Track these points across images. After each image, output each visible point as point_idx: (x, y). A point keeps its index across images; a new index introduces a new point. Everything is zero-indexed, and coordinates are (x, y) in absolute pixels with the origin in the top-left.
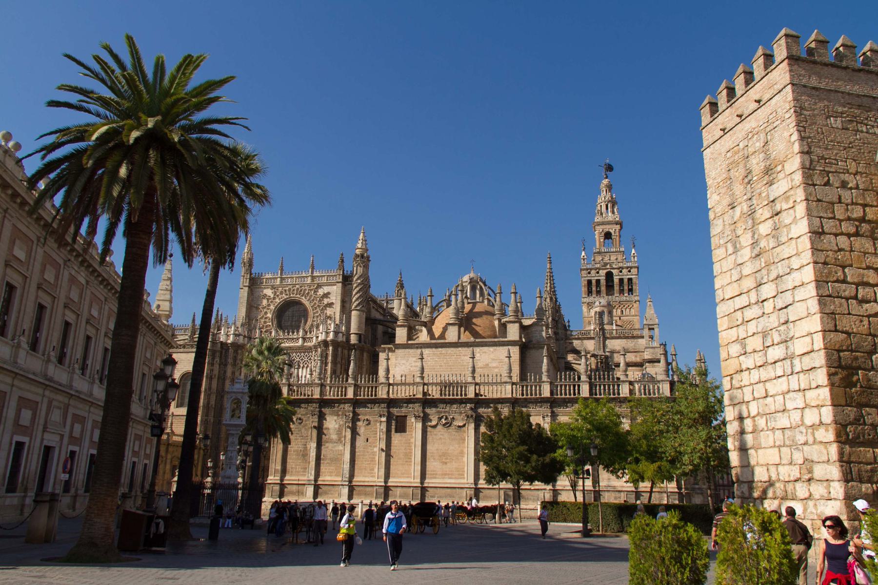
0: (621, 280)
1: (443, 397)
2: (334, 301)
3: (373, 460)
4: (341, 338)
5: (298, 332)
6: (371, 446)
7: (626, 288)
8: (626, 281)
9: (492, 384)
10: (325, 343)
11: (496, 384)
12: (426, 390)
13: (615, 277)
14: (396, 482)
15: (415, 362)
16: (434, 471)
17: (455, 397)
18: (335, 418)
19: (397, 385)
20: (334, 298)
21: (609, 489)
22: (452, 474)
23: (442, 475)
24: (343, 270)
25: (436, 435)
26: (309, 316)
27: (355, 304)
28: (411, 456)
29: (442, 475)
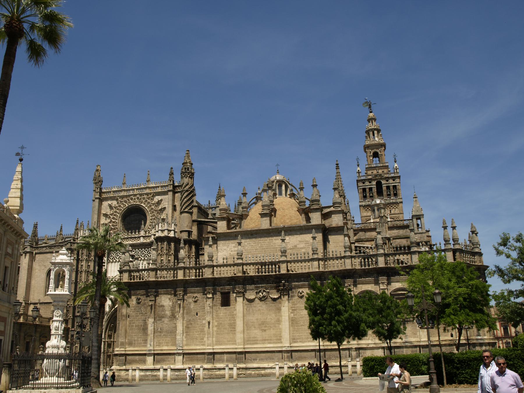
0: (388, 187)
1: (260, 274)
2: (166, 206)
3: (202, 331)
4: (172, 234)
5: (139, 232)
6: (200, 319)
7: (392, 193)
8: (391, 188)
9: (301, 261)
10: (159, 240)
11: (305, 261)
12: (245, 270)
13: (383, 185)
14: (223, 349)
15: (234, 247)
16: (255, 338)
17: (271, 274)
18: (169, 296)
19: (220, 266)
20: (167, 203)
21: (407, 344)
22: (270, 340)
23: (262, 340)
24: (173, 181)
25: (255, 307)
26: (148, 219)
27: (184, 207)
28: (235, 326)
29: (262, 340)
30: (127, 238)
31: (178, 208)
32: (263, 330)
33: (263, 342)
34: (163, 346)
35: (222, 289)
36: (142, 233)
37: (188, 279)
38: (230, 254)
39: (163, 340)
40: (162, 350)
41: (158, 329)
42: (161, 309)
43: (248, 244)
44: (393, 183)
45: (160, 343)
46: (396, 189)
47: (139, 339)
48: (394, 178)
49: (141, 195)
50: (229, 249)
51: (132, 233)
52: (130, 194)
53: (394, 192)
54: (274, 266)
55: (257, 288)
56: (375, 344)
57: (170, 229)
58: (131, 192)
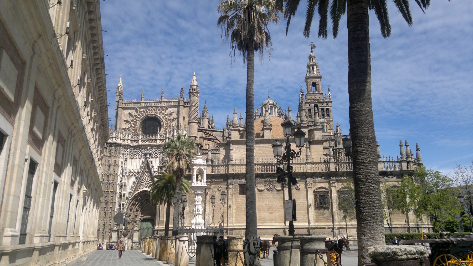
0: (323, 109)
8: (325, 110)
16: (265, 218)
22: (276, 220)
23: (270, 220)
25: (264, 195)
29: (270, 220)
30: (146, 140)
31: (187, 119)
32: (271, 212)
33: (271, 221)
35: (240, 182)
36: (159, 137)
37: (214, 174)
38: (241, 156)
41: (190, 211)
44: (327, 107)
46: (329, 111)
48: (327, 103)
49: (156, 107)
50: (240, 153)
51: (149, 136)
52: (148, 106)
53: (327, 113)
54: (273, 167)
55: (266, 182)
56: (351, 225)
58: (149, 104)
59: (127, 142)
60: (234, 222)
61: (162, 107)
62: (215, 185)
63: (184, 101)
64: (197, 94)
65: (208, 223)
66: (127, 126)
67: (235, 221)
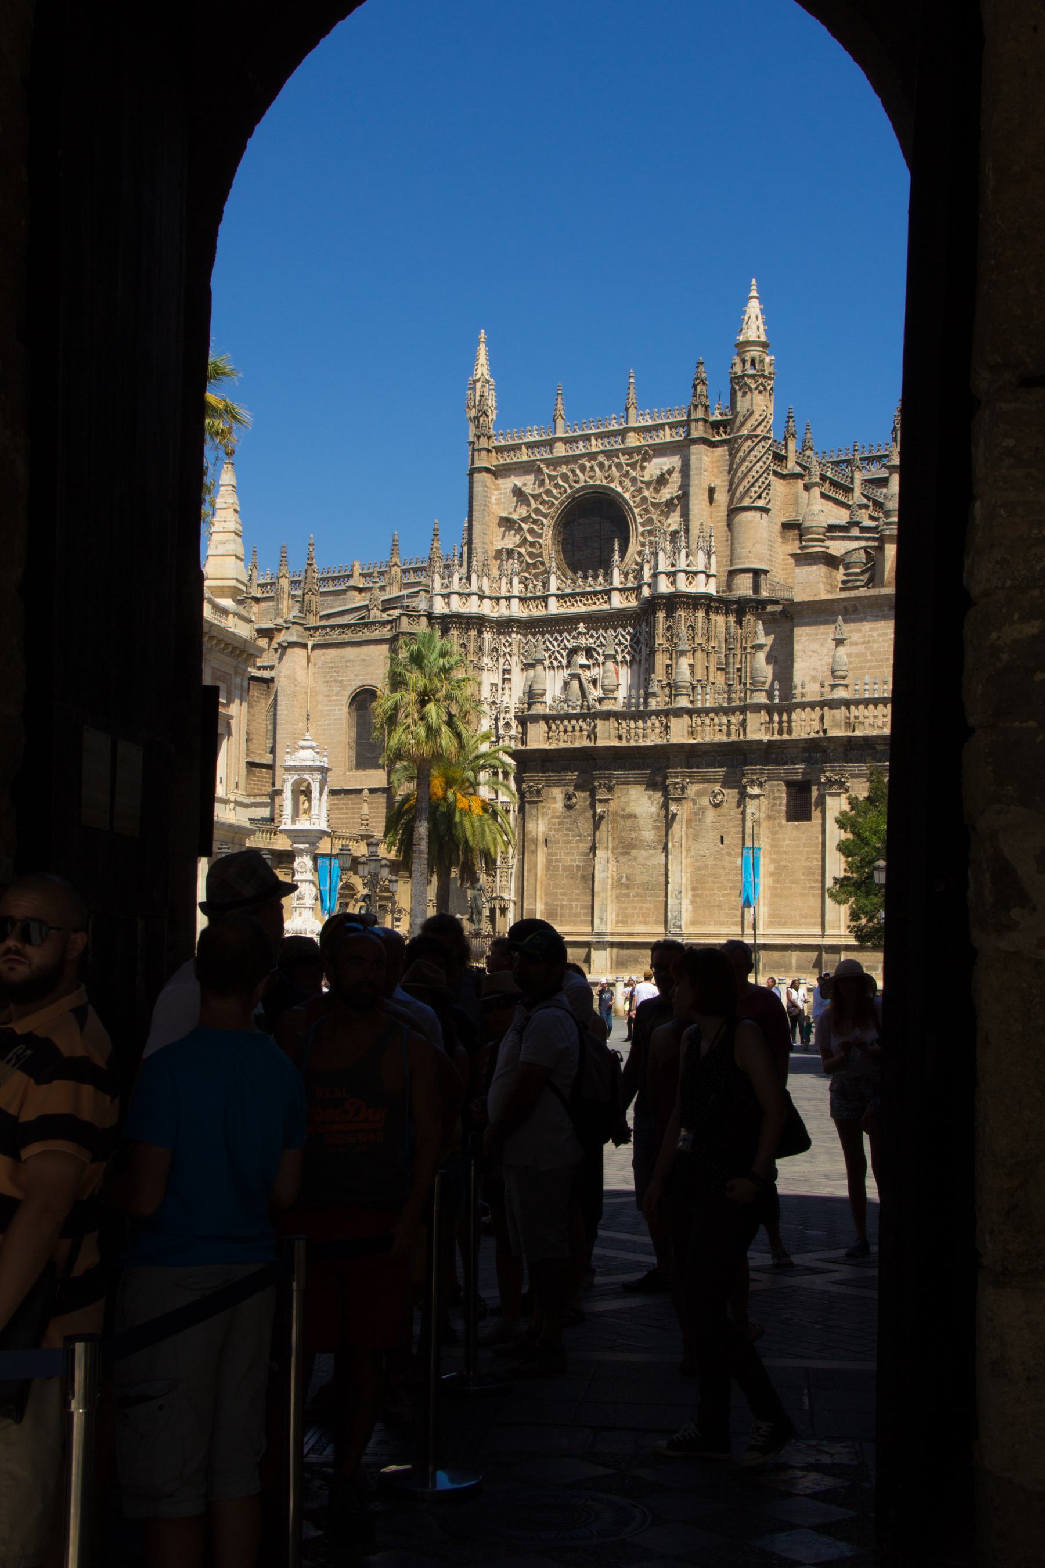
5: (608, 575)
14: (789, 936)
31: (722, 497)
34: (633, 923)
35: (787, 771)
36: (617, 579)
39: (635, 908)
40: (631, 934)
41: (622, 877)
42: (629, 823)
43: (879, 635)
45: (626, 916)
47: (574, 904)
49: (609, 454)
50: (825, 652)
51: (585, 578)
57: (693, 569)
59: (509, 607)
60: (766, 919)
61: (629, 452)
62: (701, 786)
63: (713, 418)
64: (761, 380)
65: (678, 923)
66: (511, 541)
67: (770, 916)
